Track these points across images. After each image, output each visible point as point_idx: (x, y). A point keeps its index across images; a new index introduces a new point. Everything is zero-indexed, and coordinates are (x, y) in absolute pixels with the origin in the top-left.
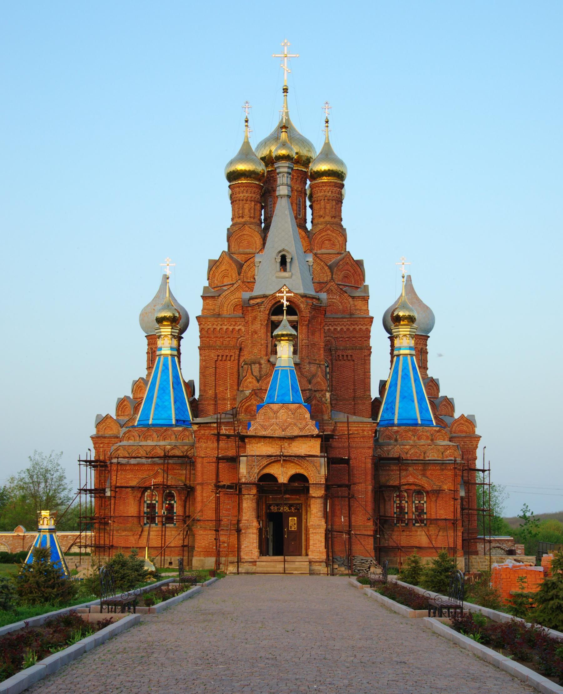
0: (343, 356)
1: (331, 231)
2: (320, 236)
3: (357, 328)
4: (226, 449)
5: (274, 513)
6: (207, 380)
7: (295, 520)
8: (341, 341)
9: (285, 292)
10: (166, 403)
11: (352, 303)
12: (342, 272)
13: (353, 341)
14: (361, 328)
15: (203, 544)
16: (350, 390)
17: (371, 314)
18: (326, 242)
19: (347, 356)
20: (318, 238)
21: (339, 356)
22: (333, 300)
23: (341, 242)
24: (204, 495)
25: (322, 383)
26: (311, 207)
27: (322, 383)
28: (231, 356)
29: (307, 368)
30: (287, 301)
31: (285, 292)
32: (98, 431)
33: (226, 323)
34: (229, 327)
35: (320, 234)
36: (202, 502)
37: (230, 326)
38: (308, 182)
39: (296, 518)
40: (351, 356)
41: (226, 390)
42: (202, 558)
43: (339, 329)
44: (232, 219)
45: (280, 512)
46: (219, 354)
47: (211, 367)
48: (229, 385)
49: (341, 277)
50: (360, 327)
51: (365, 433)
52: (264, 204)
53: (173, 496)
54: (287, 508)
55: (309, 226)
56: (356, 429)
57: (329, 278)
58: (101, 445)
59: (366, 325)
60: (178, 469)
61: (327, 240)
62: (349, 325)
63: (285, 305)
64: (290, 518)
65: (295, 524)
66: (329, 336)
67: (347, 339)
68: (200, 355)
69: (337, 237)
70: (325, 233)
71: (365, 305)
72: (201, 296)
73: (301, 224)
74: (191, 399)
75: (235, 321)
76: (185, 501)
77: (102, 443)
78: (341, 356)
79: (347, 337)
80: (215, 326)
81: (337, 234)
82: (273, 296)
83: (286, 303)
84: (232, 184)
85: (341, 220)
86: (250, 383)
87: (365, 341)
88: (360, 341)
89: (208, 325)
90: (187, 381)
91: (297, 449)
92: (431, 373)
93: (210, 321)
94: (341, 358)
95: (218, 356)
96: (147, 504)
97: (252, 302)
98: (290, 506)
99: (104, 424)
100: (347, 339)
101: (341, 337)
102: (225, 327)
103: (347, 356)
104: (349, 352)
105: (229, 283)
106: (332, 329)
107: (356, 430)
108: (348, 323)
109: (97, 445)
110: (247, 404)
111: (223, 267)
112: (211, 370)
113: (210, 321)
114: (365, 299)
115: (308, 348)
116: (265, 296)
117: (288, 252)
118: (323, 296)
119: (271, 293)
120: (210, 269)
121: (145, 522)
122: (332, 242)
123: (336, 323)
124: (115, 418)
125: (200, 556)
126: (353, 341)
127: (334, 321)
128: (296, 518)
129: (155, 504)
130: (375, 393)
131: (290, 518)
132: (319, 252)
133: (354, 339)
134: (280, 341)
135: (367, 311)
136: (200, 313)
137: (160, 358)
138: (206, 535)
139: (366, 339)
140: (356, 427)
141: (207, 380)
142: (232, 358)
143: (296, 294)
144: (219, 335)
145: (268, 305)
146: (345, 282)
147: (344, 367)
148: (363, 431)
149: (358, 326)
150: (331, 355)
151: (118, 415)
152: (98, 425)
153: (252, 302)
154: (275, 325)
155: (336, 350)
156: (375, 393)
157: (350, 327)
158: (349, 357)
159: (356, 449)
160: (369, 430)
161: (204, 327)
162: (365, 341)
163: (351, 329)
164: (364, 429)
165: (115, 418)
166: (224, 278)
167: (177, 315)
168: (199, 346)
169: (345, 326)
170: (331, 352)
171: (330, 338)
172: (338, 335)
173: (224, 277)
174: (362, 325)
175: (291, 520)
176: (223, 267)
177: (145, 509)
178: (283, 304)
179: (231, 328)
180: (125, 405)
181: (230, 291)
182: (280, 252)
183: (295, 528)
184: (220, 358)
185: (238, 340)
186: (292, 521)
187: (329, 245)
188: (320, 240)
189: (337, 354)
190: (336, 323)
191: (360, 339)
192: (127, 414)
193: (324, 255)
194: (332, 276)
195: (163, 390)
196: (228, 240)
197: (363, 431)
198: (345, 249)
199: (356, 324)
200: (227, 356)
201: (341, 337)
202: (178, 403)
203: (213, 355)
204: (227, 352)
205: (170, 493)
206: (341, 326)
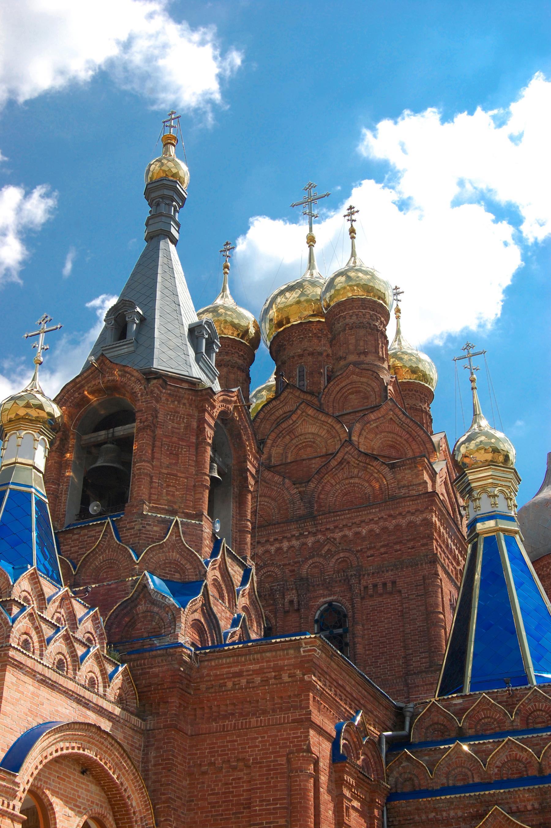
1: (357, 375)
2: (338, 389)
8: (372, 556)
11: (389, 476)
14: (411, 522)
16: (398, 660)
18: (351, 396)
19: (385, 584)
20: (335, 392)
22: (352, 481)
23: (377, 390)
25: (188, 566)
27: (188, 566)
29: (137, 527)
35: (338, 385)
50: (409, 518)
51: (285, 678)
56: (257, 667)
59: (422, 512)
61: (352, 393)
62: (386, 520)
66: (343, 551)
67: (382, 550)
69: (370, 382)
70: (348, 381)
78: (370, 586)
79: (382, 546)
81: (368, 378)
82: (77, 384)
87: (423, 545)
101: (370, 548)
104: (389, 575)
106: (350, 534)
108: (383, 514)
115: (151, 482)
122: (362, 394)
127: (350, 518)
133: (398, 547)
139: (425, 541)
140: (257, 662)
147: (381, 611)
148: (279, 669)
150: (350, 588)
158: (389, 585)
160: (295, 666)
162: (423, 545)
163: (391, 527)
164: (280, 663)
169: (376, 523)
171: (347, 554)
174: (413, 514)
187: (357, 401)
188: (339, 395)
189: (363, 583)
191: (410, 544)
193: (346, 417)
197: (279, 669)
206: (368, 524)
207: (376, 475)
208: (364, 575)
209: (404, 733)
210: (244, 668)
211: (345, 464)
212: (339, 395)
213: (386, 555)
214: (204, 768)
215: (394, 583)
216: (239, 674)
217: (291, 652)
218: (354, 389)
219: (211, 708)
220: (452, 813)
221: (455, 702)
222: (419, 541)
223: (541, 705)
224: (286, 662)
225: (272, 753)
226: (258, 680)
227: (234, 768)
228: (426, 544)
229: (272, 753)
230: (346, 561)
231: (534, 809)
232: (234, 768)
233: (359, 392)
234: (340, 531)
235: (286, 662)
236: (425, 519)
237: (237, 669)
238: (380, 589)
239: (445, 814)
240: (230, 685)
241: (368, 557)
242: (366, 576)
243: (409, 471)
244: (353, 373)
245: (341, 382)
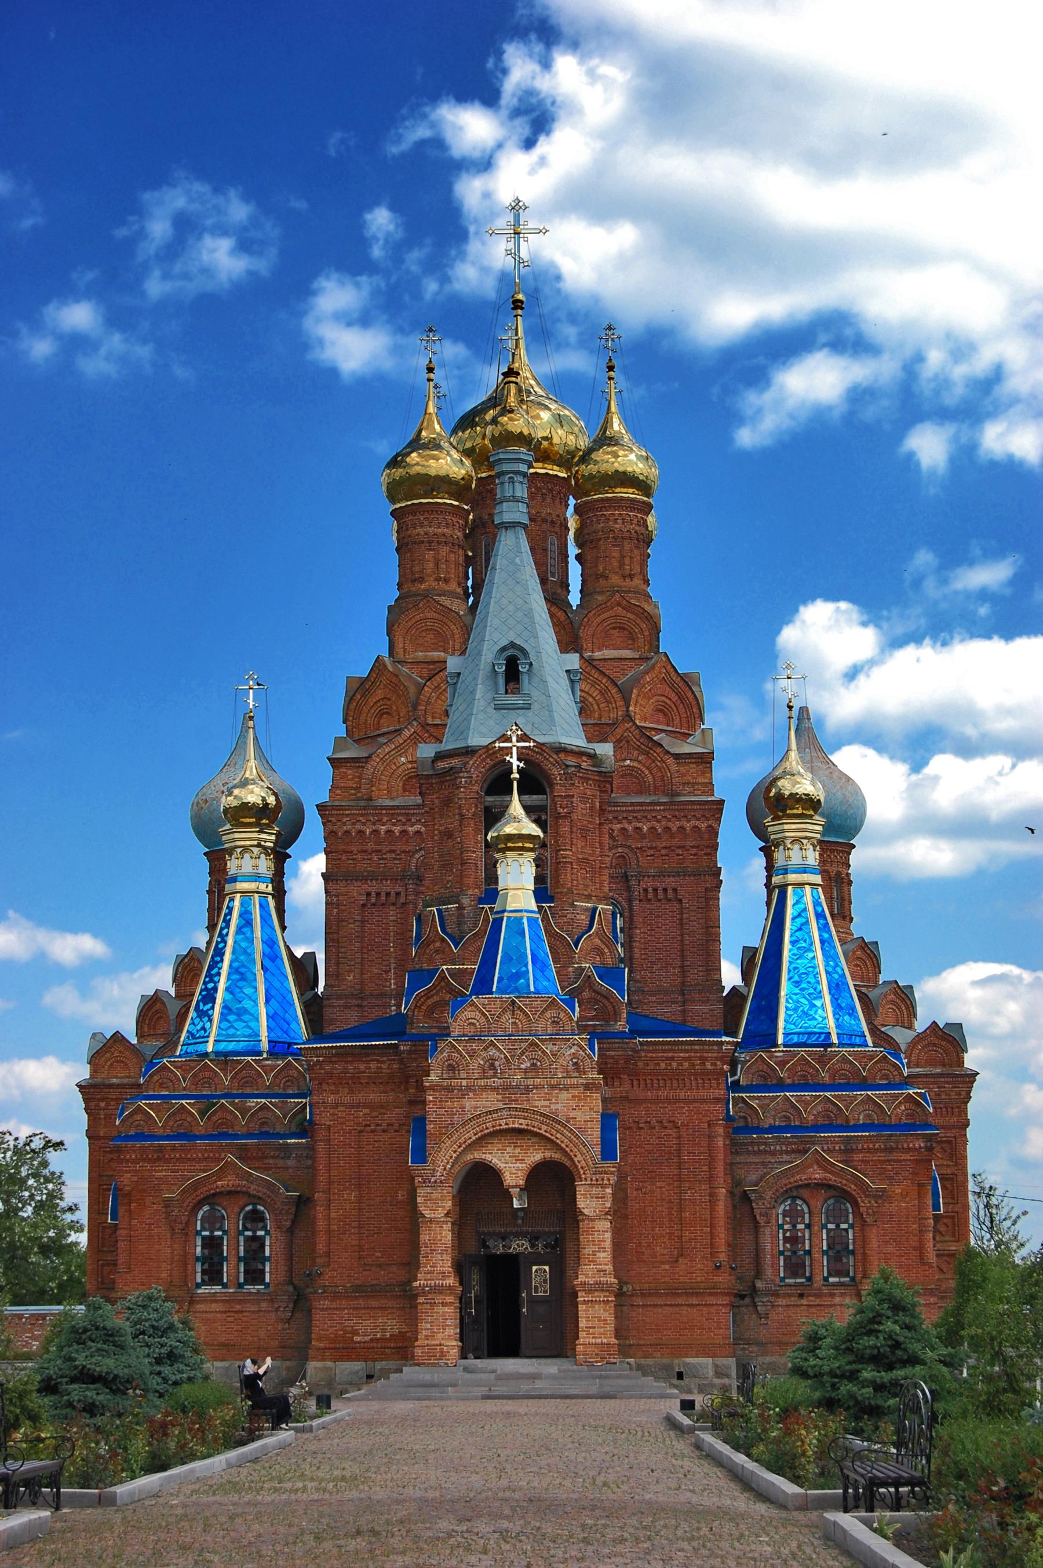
0: (655, 890)
1: (623, 608)
2: (599, 620)
3: (688, 826)
4: (382, 1107)
5: (495, 1256)
6: (343, 950)
7: (545, 1271)
8: (651, 856)
9: (514, 739)
10: (247, 1004)
11: (674, 768)
12: (649, 698)
13: (678, 855)
15: (331, 1330)
16: (674, 968)
17: (718, 795)
18: (612, 632)
19: (665, 890)
20: (595, 624)
21: (646, 890)
24: (333, 1215)
25: (606, 951)
26: (578, 557)
27: (606, 951)
28: (398, 894)
29: (569, 916)
30: (519, 759)
31: (514, 739)
32: (94, 1072)
33: (385, 819)
34: (393, 828)
36: (329, 1232)
37: (394, 824)
38: (572, 501)
39: (547, 1268)
40: (675, 890)
41: (387, 972)
42: (329, 1364)
43: (645, 829)
44: (400, 586)
45: (511, 1255)
46: (370, 889)
47: (352, 921)
48: (392, 960)
49: (649, 709)
51: (708, 1065)
52: (470, 554)
53: (262, 1219)
54: (527, 1244)
55: (574, 598)
57: (620, 713)
58: (103, 1104)
60: (272, 1157)
61: (614, 628)
62: (669, 820)
63: (515, 768)
64: (534, 1268)
65: (545, 1281)
66: (622, 846)
67: (663, 852)
68: (327, 892)
69: (638, 621)
71: (703, 773)
72: (328, 758)
73: (555, 597)
74: (309, 995)
75: (407, 814)
76: (291, 1231)
77: (102, 1100)
78: (650, 890)
79: (665, 848)
80: (358, 827)
81: (637, 615)
83: (515, 763)
84: (398, 506)
85: (647, 582)
86: (437, 951)
87: (706, 854)
88: (695, 855)
89: (344, 824)
90: (299, 953)
91: (547, 1103)
92: (858, 928)
93: (347, 816)
94: (650, 896)
95: (368, 894)
96: (204, 1238)
97: (442, 765)
98: (533, 1239)
99: (108, 1055)
100: (663, 852)
101: (651, 848)
102: (383, 829)
103: (665, 890)
104: (670, 882)
105: (391, 728)
107: (685, 1059)
108: (667, 814)
109: (92, 1104)
110: (430, 1002)
111: (380, 694)
112: (352, 926)
113: (347, 816)
114: (705, 760)
116: (469, 752)
117: (523, 650)
118: (605, 750)
119: (485, 742)
120: (350, 699)
121: (199, 1280)
122: (626, 632)
123: (639, 815)
124: (134, 1041)
125: (323, 1360)
126: (678, 855)
127: (632, 811)
128: (547, 1268)
129: (221, 1238)
130: (730, 975)
131: (534, 1268)
132: (598, 655)
134: (503, 851)
135: (709, 787)
136: (325, 797)
137: (232, 900)
138: (336, 1309)
141: (343, 950)
142: (402, 900)
143: (540, 745)
144: (370, 846)
145: (476, 771)
146: (658, 722)
147: (658, 917)
149: (688, 821)
150: (629, 889)
151: (140, 1034)
152: (95, 1060)
153: (442, 765)
154: (493, 816)
155: (641, 876)
156: (730, 975)
157: (670, 824)
158: (670, 891)
159: (685, 1103)
160: (716, 1058)
161: (335, 828)
162: (706, 854)
163: (674, 829)
165: (134, 1041)
166: (381, 717)
167: (271, 800)
168: (324, 871)
169: (659, 821)
170: (627, 881)
171: (626, 850)
172: (645, 843)
173: (381, 714)
174: (698, 819)
175: (536, 1271)
176: (380, 694)
177: (199, 1249)
178: (511, 764)
179: (397, 830)
180: (157, 1012)
181: (393, 747)
182: (503, 649)
183: (545, 1292)
184: (373, 900)
185: (412, 857)
186: (539, 1274)
187: (619, 640)
188: (600, 628)
190: (639, 815)
192: (160, 1032)
193: (609, 662)
194: (628, 708)
195: (240, 974)
196: (389, 633)
197: (703, 1060)
198: (658, 647)
199: (686, 817)
200: (388, 894)
201: (651, 848)
202: (273, 1002)
203: (356, 891)
204: (388, 887)
205: (255, 1211)
207: (659, 764)
208: (644, 876)
209: (736, 1077)
210: (676, 1055)
211: (624, 742)
212: (600, 628)
213: (667, 858)
214: (641, 1125)
215: (675, 890)
216: (672, 1059)
217: (715, 1048)
218: (618, 625)
219: (645, 1080)
220: (778, 1148)
221: (776, 1054)
222: (702, 850)
223: (847, 1066)
224: (710, 1055)
225: (696, 1119)
226: (686, 1065)
227: (666, 1128)
228: (710, 854)
229: (696, 1119)
230: (624, 857)
231: (840, 1149)
232: (666, 1128)
233: (624, 629)
234: (619, 823)
235: (710, 1055)
236: (710, 826)
237: (670, 1055)
238: (661, 895)
239: (772, 1147)
240: (663, 1065)
241: (648, 856)
242: (646, 878)
243: (695, 766)
244: (619, 604)
245: (603, 613)
